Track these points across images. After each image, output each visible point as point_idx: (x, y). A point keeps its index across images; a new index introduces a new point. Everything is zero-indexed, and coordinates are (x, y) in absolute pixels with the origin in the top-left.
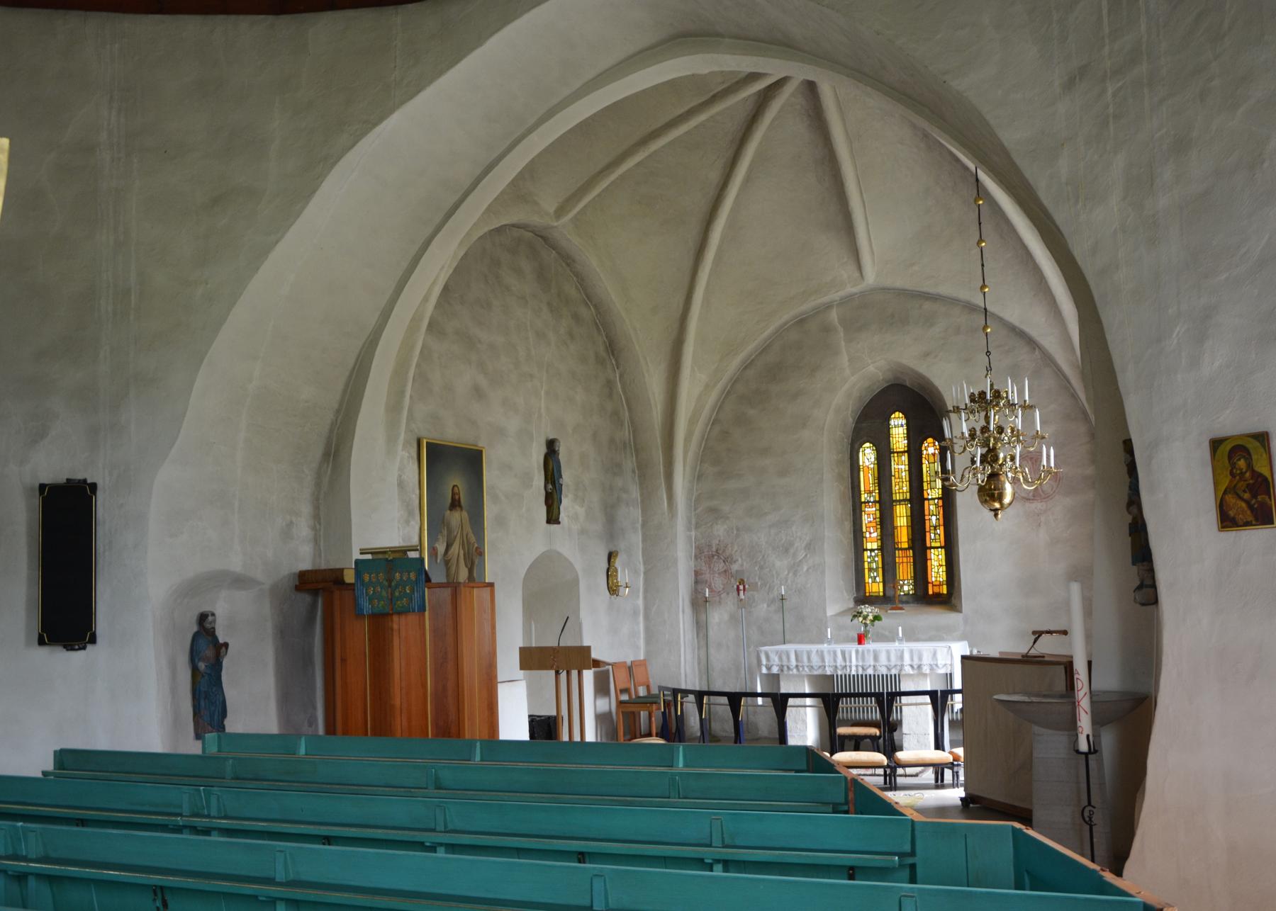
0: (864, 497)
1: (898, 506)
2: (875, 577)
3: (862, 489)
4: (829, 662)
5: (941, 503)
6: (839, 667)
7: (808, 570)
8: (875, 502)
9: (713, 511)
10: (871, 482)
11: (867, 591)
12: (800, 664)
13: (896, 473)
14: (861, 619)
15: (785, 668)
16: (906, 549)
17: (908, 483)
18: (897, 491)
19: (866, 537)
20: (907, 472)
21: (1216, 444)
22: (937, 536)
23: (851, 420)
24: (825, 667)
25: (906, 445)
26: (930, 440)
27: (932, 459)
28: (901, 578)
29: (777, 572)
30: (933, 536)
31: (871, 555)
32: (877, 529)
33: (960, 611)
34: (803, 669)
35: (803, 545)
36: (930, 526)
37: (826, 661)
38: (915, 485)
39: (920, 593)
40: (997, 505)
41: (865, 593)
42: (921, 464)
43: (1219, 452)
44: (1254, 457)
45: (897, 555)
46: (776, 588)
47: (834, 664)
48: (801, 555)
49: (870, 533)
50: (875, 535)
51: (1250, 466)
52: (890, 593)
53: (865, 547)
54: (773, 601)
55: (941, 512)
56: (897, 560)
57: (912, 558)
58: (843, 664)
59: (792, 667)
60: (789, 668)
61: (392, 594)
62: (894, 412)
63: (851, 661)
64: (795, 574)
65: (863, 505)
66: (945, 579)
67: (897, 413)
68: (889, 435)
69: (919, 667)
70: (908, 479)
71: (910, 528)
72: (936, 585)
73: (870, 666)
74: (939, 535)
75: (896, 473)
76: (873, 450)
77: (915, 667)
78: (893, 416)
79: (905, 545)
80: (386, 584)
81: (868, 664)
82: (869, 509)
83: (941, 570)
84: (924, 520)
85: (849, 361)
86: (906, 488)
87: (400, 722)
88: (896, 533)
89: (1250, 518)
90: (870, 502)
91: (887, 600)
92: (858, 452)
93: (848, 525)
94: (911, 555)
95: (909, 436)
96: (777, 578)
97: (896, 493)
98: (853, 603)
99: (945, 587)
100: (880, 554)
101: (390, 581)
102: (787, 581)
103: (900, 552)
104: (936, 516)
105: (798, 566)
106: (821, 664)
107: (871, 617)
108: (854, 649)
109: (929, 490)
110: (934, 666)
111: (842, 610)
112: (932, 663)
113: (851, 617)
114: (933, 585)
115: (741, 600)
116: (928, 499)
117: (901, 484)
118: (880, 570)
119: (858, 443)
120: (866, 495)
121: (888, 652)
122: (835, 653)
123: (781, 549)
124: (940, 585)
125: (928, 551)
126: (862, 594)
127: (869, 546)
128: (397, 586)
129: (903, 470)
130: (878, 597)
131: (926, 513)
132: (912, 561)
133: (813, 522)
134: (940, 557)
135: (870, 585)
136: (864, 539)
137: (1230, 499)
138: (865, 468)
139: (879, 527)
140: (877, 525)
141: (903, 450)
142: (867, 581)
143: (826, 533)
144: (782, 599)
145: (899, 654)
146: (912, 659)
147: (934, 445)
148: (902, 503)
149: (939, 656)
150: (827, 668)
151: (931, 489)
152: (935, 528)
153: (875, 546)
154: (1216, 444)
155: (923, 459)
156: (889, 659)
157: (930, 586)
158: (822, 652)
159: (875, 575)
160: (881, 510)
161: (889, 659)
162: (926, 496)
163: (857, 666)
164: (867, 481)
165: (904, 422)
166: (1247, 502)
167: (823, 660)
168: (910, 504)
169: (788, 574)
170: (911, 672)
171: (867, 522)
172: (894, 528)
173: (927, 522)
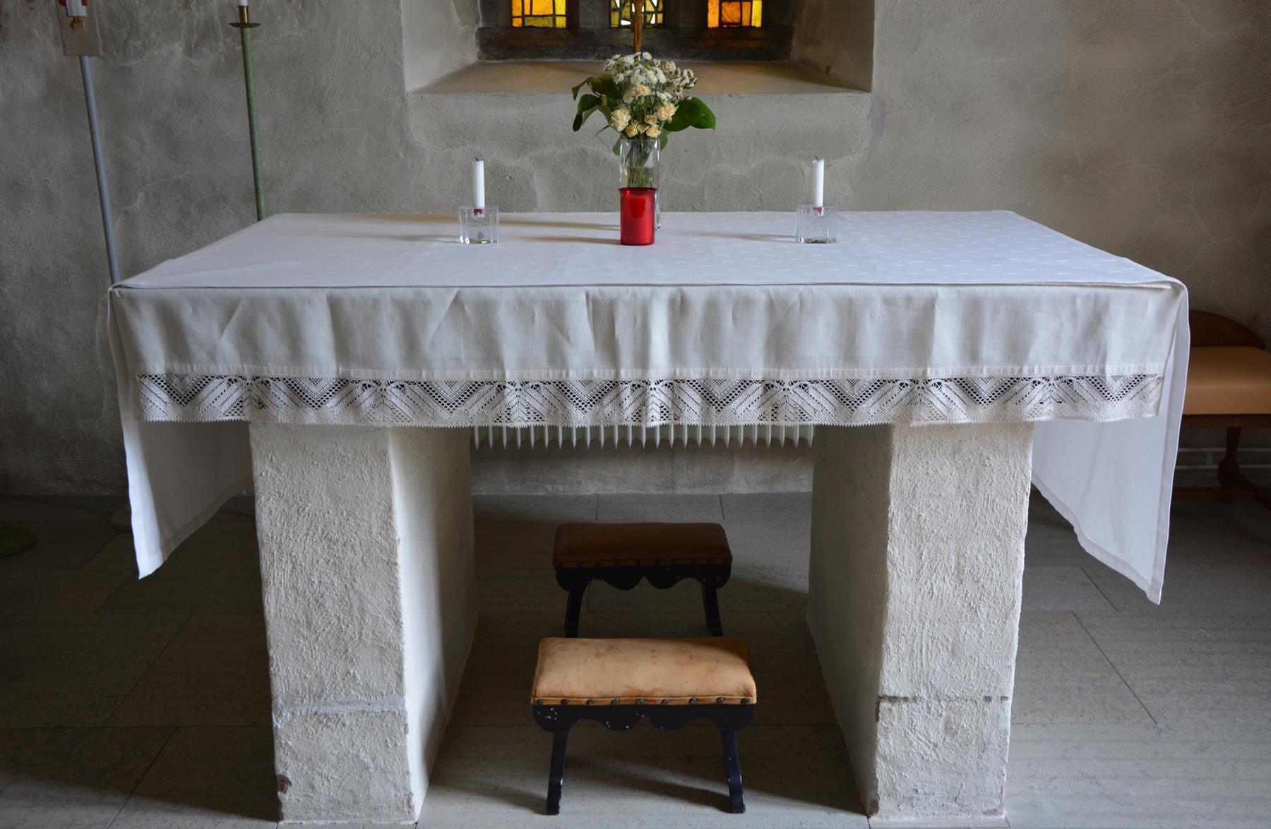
4: (523, 363)
11: (517, 11)
12: (360, 373)
14: (622, 117)
15: (280, 394)
24: (501, 388)
33: (864, 87)
34: (381, 397)
37: (510, 355)
41: (511, 17)
47: (552, 375)
52: (590, 20)
54: (206, 33)
58: (602, 374)
59: (315, 391)
60: (297, 394)
63: (643, 358)
69: (1008, 389)
73: (745, 384)
81: (736, 376)
98: (477, 50)
106: (476, 374)
107: (668, 112)
108: (665, 294)
110: (1084, 388)
111: (447, 71)
112: (1075, 371)
113: (571, 107)
115: (77, 20)
121: (849, 315)
122: (557, 314)
130: (551, 31)
144: (242, 25)
145: (906, 322)
146: (972, 352)
149: (1116, 337)
150: (511, 397)
156: (849, 349)
158: (486, 309)
161: (849, 349)
163: (674, 385)
167: (490, 350)
170: (961, 415)
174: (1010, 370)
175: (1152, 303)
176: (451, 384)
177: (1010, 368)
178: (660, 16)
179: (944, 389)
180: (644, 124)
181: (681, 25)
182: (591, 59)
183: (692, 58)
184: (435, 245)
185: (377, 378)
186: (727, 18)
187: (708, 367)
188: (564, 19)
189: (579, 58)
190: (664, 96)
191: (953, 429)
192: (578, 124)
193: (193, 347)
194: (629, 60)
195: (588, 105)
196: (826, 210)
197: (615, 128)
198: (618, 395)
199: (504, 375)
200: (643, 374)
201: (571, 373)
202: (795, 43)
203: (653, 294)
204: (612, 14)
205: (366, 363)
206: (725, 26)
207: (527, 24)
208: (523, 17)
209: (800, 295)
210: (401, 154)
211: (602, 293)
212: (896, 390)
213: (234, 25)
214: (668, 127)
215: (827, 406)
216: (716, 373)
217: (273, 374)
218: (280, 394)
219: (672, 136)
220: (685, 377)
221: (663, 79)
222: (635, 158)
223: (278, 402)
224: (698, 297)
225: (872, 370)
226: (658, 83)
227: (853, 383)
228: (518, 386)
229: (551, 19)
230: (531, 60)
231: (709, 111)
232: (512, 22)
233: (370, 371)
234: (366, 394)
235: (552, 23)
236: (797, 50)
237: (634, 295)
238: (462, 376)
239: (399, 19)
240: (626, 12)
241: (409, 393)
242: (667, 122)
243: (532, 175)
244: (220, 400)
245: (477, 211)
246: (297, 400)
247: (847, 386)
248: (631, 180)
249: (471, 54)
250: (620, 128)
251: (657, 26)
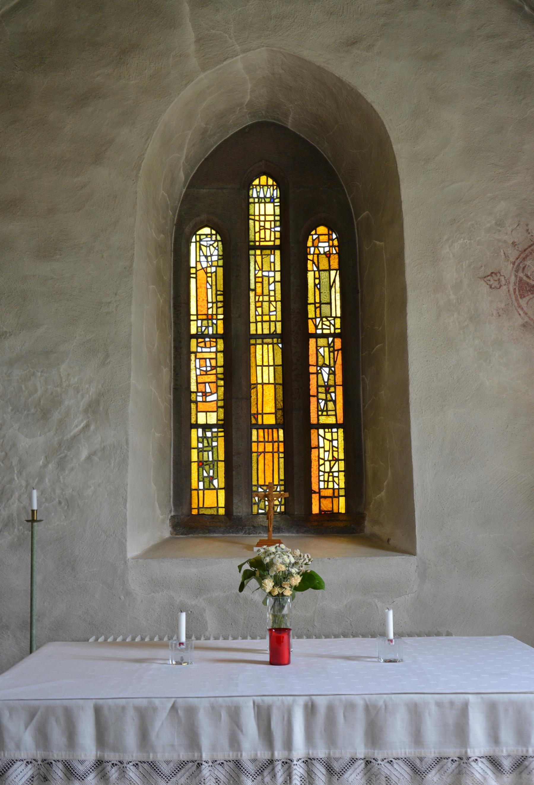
1: (259, 347)
2: (212, 479)
3: (193, 311)
4: (214, 748)
5: (338, 343)
6: (251, 768)
7: (89, 458)
8: (216, 336)
10: (210, 300)
11: (195, 505)
12: (111, 756)
13: (259, 285)
14: (269, 584)
16: (270, 427)
17: (279, 304)
18: (259, 318)
19: (196, 402)
20: (278, 285)
22: (331, 405)
23: (182, 176)
24: (199, 765)
25: (278, 235)
26: (322, 230)
27: (324, 264)
28: (261, 482)
29: (20, 461)
30: (322, 404)
31: (204, 437)
32: (217, 386)
33: (412, 553)
34: (123, 772)
35: (83, 404)
36: (318, 386)
37: (205, 742)
38: (294, 306)
39: (297, 511)
41: (191, 509)
42: (306, 271)
45: (254, 438)
46: (17, 494)
47: (232, 756)
49: (205, 394)
52: (239, 510)
53: (193, 421)
56: (254, 448)
57: (282, 445)
58: (263, 755)
59: (81, 769)
62: (259, 176)
63: (288, 744)
64: (61, 465)
65: (193, 342)
66: (342, 485)
67: (263, 179)
68: (249, 215)
70: (279, 297)
71: (280, 389)
72: (325, 497)
73: (353, 760)
74: (335, 402)
75: (259, 285)
76: (216, 240)
77: (507, 764)
78: (256, 182)
79: (270, 420)
81: (347, 755)
82: (204, 350)
83: (335, 469)
85: (198, 41)
86: (276, 314)
88: (253, 397)
90: (208, 336)
92: (189, 242)
94: (281, 438)
96: (20, 473)
97: (256, 322)
98: (170, 529)
99: (342, 500)
100: (222, 434)
102: (41, 478)
103: (261, 432)
104: (329, 366)
105: (69, 448)
106: (184, 756)
107: (296, 580)
108: (301, 701)
109: (318, 320)
111: (152, 543)
113: (239, 577)
114: (321, 497)
116: (316, 336)
117: (266, 305)
118: (221, 465)
119: (191, 224)
120: (199, 322)
123: (33, 411)
124: (334, 496)
125: (314, 432)
126: (185, 511)
127: (202, 419)
129: (272, 280)
131: (312, 360)
132: (282, 449)
133: (107, 356)
134: (335, 443)
135: (201, 493)
136: (193, 406)
138: (201, 274)
139: (222, 383)
140: (218, 379)
141: (271, 243)
142: (194, 485)
143: (133, 381)
144: (33, 521)
145: (451, 717)
147: (330, 239)
148: (266, 341)
150: (206, 771)
151: (321, 318)
152: (327, 387)
153: (212, 419)
155: (310, 263)
157: (315, 498)
159: (211, 474)
162: (311, 329)
163: (308, 761)
164: (202, 296)
165: (276, 193)
168: (282, 343)
169: (45, 466)
171: (198, 373)
172: (250, 386)
173: (313, 378)
174: (520, 751)
176: (168, 762)
177: (520, 749)
178: (283, 507)
179: (480, 764)
180: (281, 587)
181: (296, 513)
182: (241, 535)
183: (303, 533)
184: (155, 666)
185: (121, 759)
186: (324, 508)
187: (329, 749)
188: (224, 509)
189: (233, 533)
190: (294, 570)
192: (242, 587)
193: (7, 740)
194: (272, 549)
195: (248, 575)
196: (395, 641)
197: (265, 590)
198: (273, 769)
199: (201, 756)
200: (289, 754)
201: (244, 754)
202: (366, 523)
203: (294, 701)
204: (253, 506)
205: (115, 749)
206: (323, 513)
207: (201, 512)
208: (198, 508)
209: (385, 702)
210: (122, 597)
211: (263, 701)
212: (449, 764)
213: (28, 521)
214: (296, 589)
215: (407, 776)
216: (334, 753)
217: (56, 758)
218: (58, 771)
219: (298, 594)
220: (315, 756)
221: (293, 560)
222: (277, 608)
223: (57, 777)
224: (321, 703)
225: (433, 750)
226: (290, 563)
227: (421, 759)
228: (210, 764)
229: (215, 509)
230: (203, 535)
231: (321, 579)
232: (191, 511)
233: (117, 754)
234: (113, 770)
235: (216, 512)
236: (368, 527)
237: (283, 702)
238: (175, 757)
239: (126, 514)
240: (262, 505)
241: (141, 769)
242: (295, 586)
243: (205, 610)
244: (19, 777)
245: (182, 644)
246: (69, 775)
247: (418, 762)
248: (274, 622)
249: (166, 532)
250: (268, 591)
251: (281, 513)
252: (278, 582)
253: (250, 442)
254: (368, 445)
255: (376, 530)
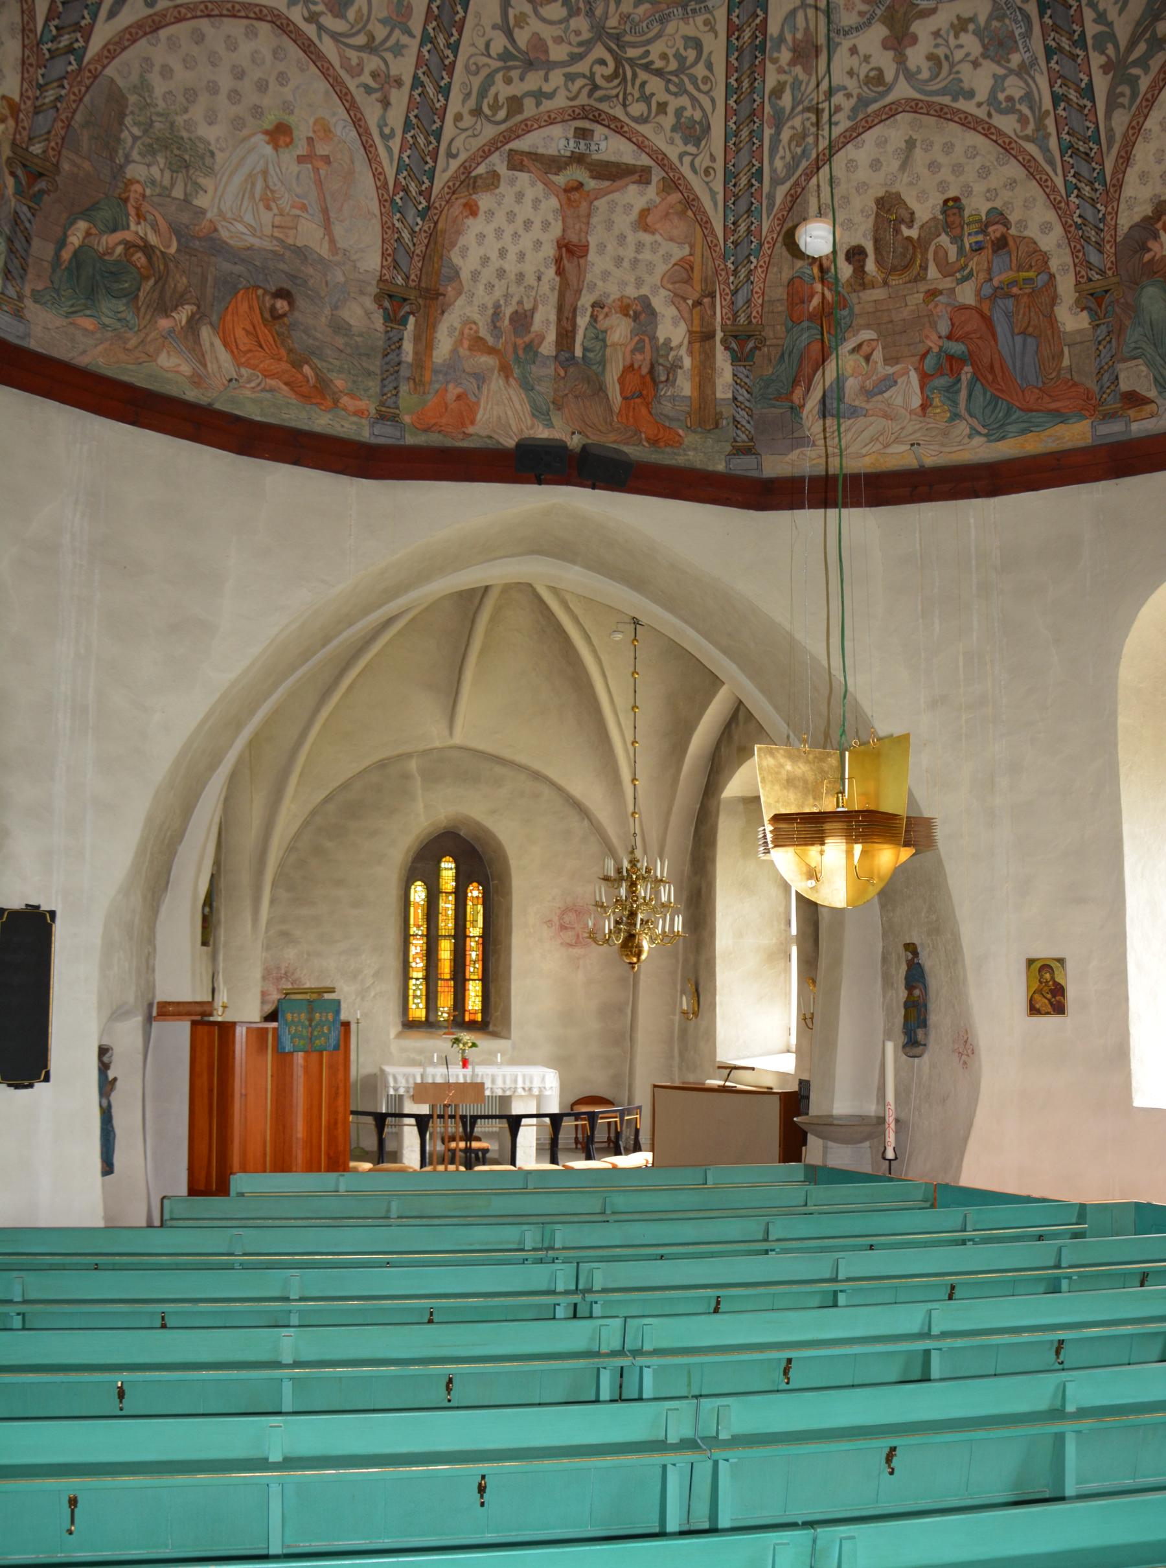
0: (413, 930)
3: (412, 922)
5: (481, 941)
7: (374, 997)
8: (422, 935)
9: (285, 934)
14: (461, 1046)
16: (447, 980)
21: (1030, 962)
27: (475, 901)
40: (635, 960)
43: (1032, 967)
44: (1056, 973)
48: (369, 982)
50: (421, 965)
51: (1053, 978)
52: (432, 1019)
55: (481, 949)
61: (312, 1033)
64: (363, 999)
65: (412, 938)
69: (530, 1089)
79: (447, 976)
80: (307, 1023)
84: (465, 955)
86: (451, 925)
87: (299, 1154)
89: (1050, 1009)
91: (429, 1024)
92: (410, 888)
93: (401, 954)
95: (457, 878)
101: (311, 1020)
107: (470, 1044)
118: (424, 998)
121: (504, 1077)
124: (476, 1013)
127: (415, 976)
128: (316, 1026)
130: (420, 1022)
131: (468, 948)
137: (1037, 997)
152: (475, 962)
154: (1030, 962)
156: (504, 1082)
157: (467, 1014)
160: (428, 943)
161: (504, 1082)
166: (1049, 1000)
172: (438, 960)
173: (468, 957)
175: (552, 1075)
191: (521, 1096)
195: (454, 1043)
236: (491, 1028)
252: (464, 1044)
253: (437, 986)
254: (492, 990)
255: (495, 1029)
